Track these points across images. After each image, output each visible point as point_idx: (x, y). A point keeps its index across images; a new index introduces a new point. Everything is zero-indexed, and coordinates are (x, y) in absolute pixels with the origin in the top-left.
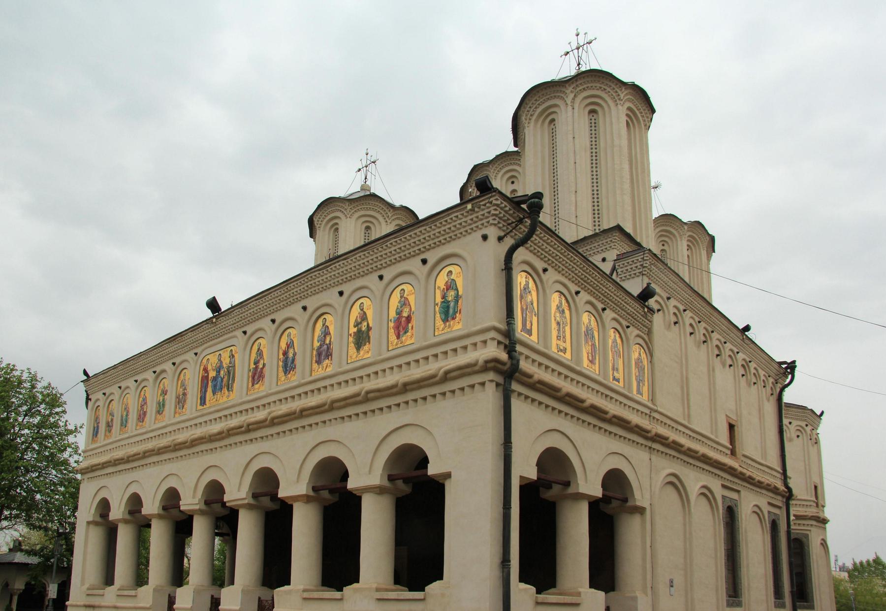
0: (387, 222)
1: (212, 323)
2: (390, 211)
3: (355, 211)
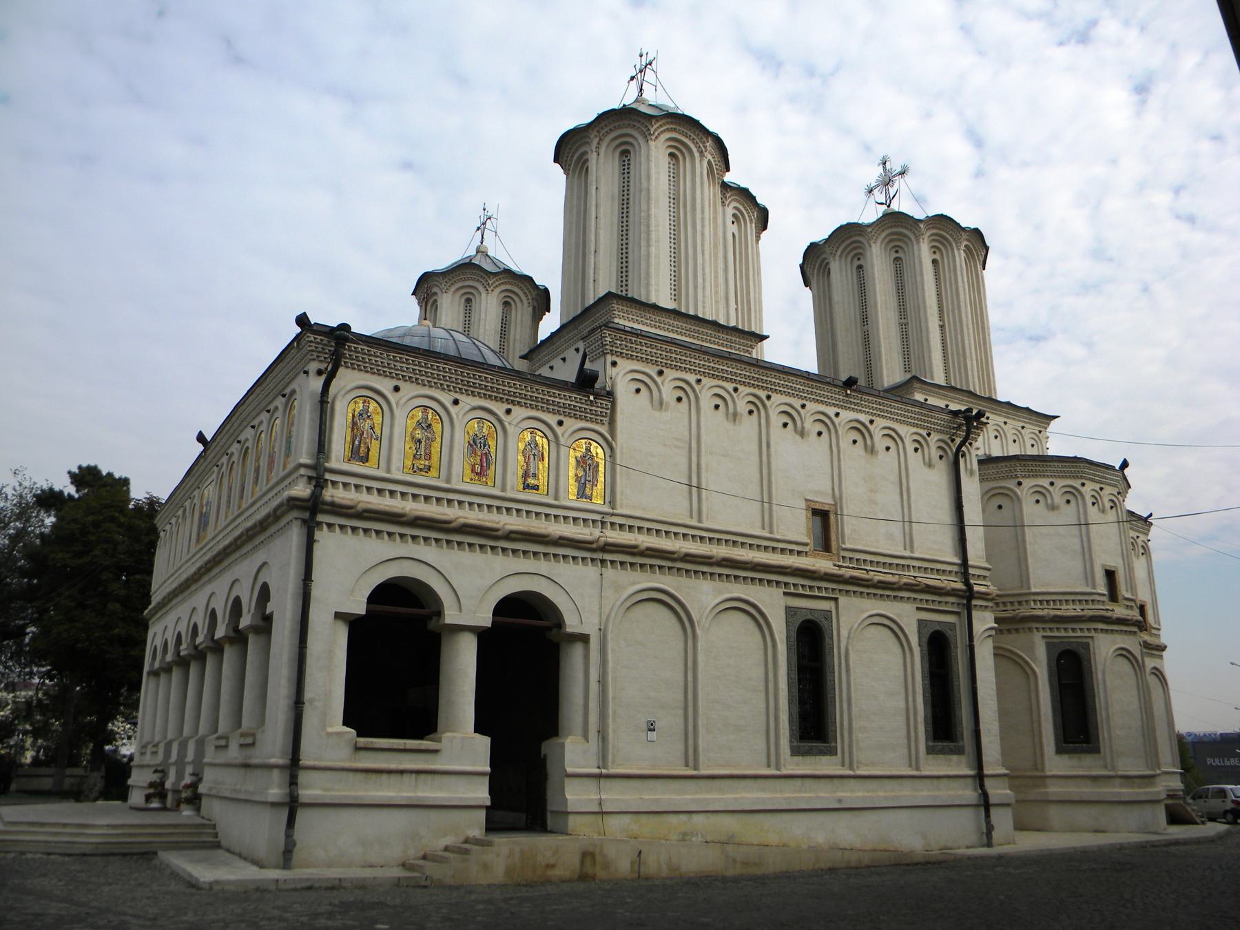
0: (487, 290)
1: (203, 457)
2: (489, 277)
3: (452, 284)
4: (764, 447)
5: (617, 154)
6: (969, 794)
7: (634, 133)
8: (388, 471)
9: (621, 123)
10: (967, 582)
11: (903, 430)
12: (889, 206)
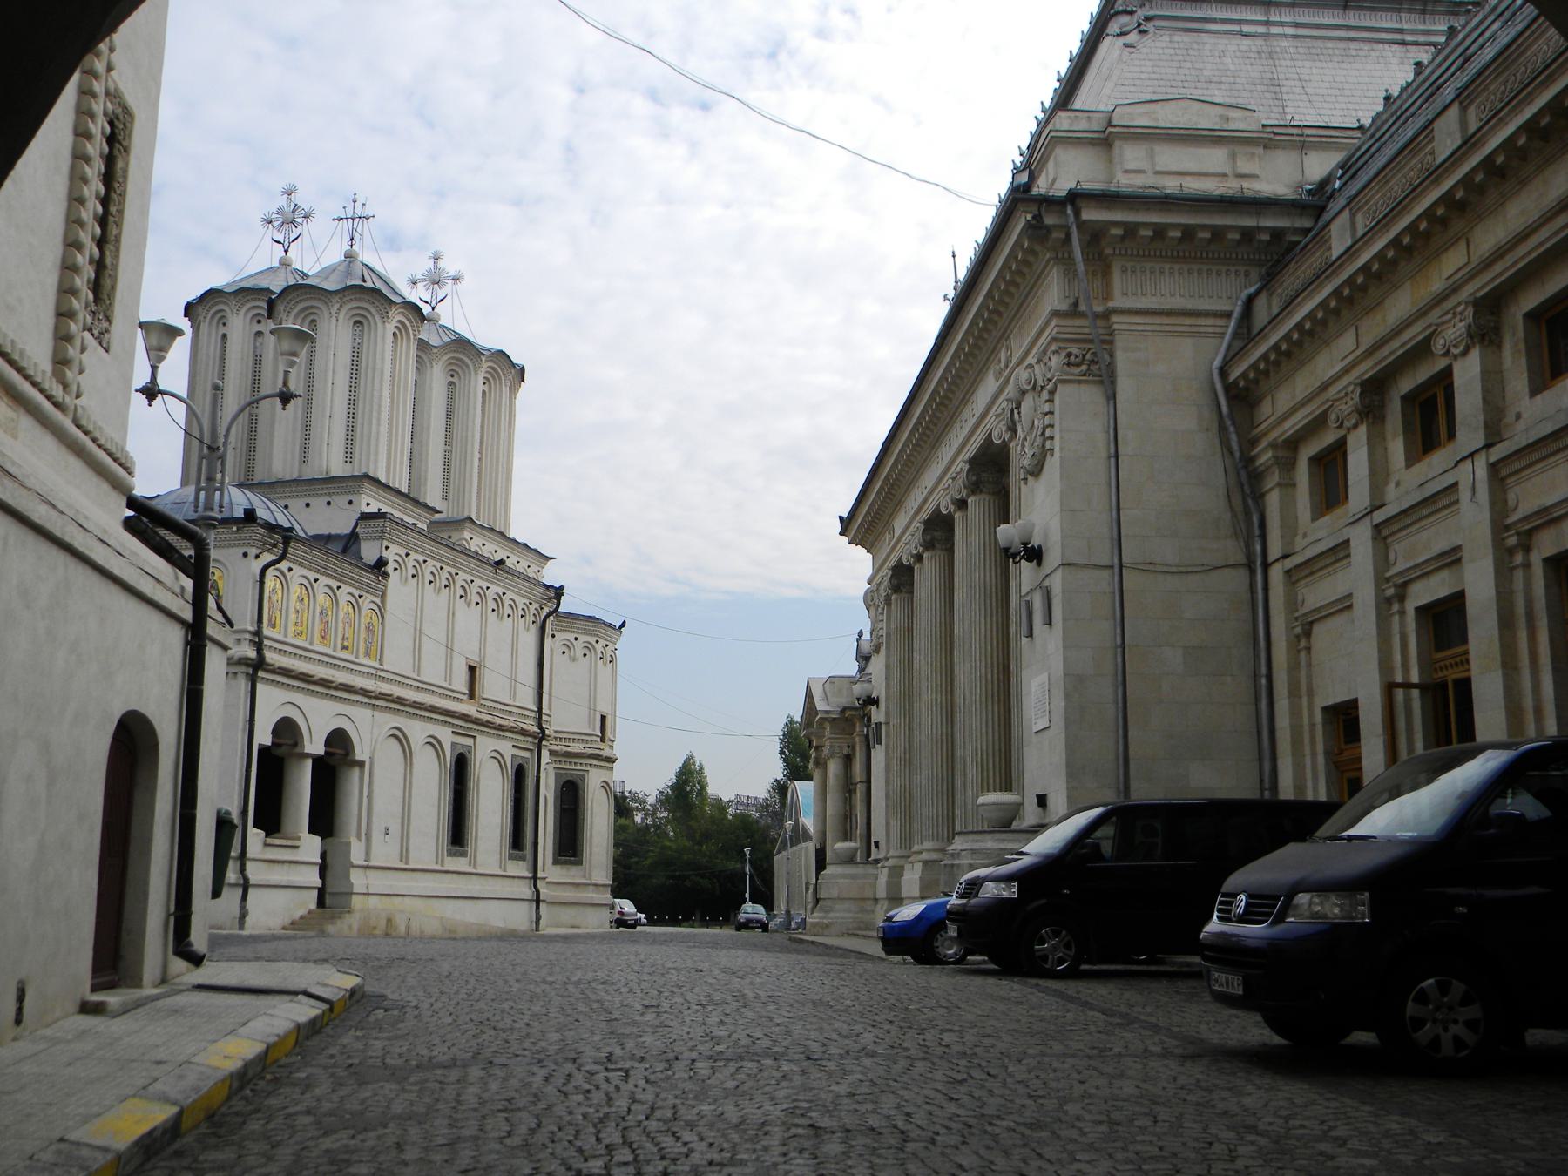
4: (451, 614)
5: (351, 324)
6: (528, 892)
7: (372, 310)
8: (286, 636)
9: (362, 296)
10: (540, 727)
11: (521, 602)
12: (433, 308)
